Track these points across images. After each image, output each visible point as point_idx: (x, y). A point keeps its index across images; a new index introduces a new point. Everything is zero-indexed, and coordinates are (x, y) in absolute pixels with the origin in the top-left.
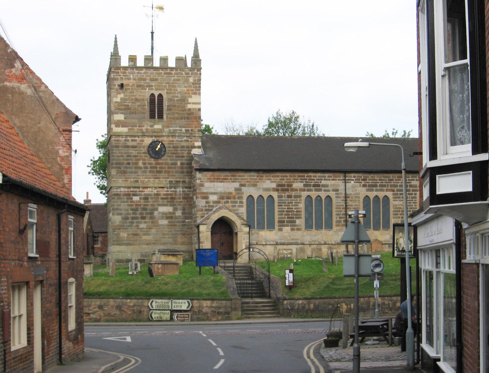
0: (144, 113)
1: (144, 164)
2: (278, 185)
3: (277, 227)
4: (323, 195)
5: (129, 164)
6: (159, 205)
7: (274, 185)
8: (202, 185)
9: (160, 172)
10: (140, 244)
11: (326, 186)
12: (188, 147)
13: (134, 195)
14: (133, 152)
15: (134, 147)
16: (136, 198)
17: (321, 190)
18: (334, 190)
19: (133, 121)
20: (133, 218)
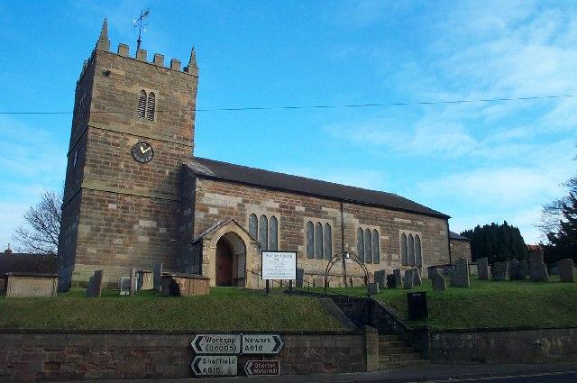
0: (132, 110)
1: (126, 166)
2: (282, 206)
6: (141, 218)
7: (277, 206)
8: (203, 196)
9: (146, 179)
10: (113, 264)
11: (326, 213)
12: (178, 156)
14: (112, 148)
15: (114, 145)
16: (112, 206)
20: (106, 230)
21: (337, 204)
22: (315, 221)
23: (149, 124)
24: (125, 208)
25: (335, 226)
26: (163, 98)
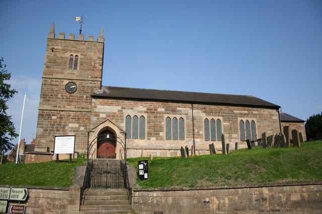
3: (146, 138)
4: (178, 117)
5: (52, 95)
6: (69, 122)
7: (145, 109)
8: (96, 107)
9: (72, 101)
12: (91, 87)
13: (53, 115)
14: (56, 88)
15: (56, 85)
16: (54, 118)
17: (176, 114)
18: (185, 114)
19: (58, 69)
20: (51, 130)
21: (190, 105)
22: (172, 116)
23: (75, 72)
24: (61, 118)
25: (187, 118)
26: (83, 57)
